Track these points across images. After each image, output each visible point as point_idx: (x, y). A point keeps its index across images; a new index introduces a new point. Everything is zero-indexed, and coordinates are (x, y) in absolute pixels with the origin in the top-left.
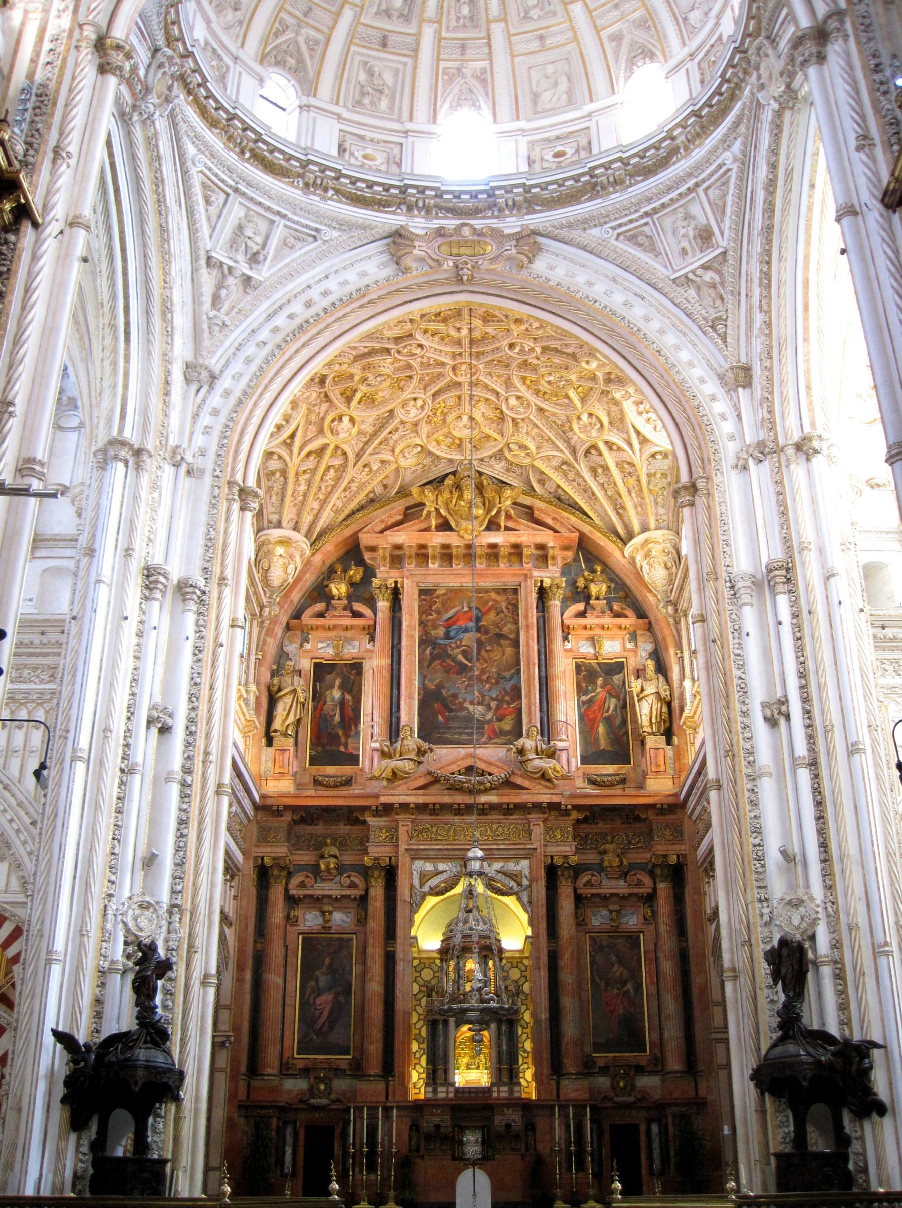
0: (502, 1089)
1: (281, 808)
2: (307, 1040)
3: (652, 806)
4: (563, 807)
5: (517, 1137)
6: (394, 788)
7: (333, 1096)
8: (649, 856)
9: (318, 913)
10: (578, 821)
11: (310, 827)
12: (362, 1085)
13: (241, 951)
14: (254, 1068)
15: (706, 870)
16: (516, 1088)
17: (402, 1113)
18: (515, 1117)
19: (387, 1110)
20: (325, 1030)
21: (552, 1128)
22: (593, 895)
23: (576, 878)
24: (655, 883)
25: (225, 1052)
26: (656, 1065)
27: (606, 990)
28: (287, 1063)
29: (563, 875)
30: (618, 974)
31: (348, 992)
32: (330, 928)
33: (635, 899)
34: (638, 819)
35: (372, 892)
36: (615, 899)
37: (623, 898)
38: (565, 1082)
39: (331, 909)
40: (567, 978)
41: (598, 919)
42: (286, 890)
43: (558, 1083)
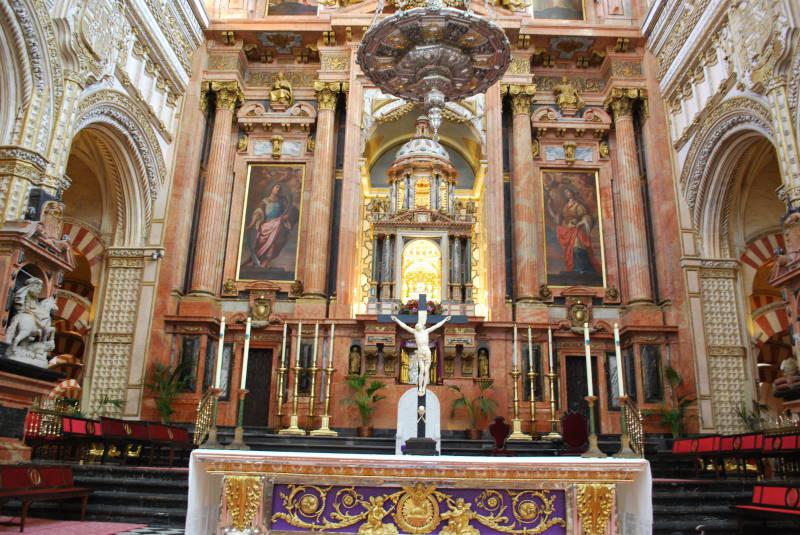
0: (454, 307)
1: (231, 33)
2: (251, 264)
3: (613, 41)
4: (521, 37)
5: (468, 360)
6: (345, 12)
7: (271, 317)
8: (604, 98)
9: (268, 143)
10: (535, 62)
11: (264, 65)
12: (301, 303)
13: (180, 167)
14: (188, 288)
15: (671, 100)
16: (469, 307)
17: (342, 333)
18: (468, 339)
19: (325, 328)
20: (269, 255)
21: (508, 354)
22: (551, 130)
23: (531, 111)
24: (613, 120)
25: (155, 263)
26: (615, 297)
27: (561, 224)
28: (227, 285)
29: (519, 104)
30: (572, 209)
31: (294, 217)
32: (279, 156)
33: (590, 137)
34: (596, 62)
35: (321, 116)
36: (571, 136)
37: (578, 134)
38: (520, 306)
39: (280, 137)
40: (523, 201)
41: (554, 154)
42: (235, 122)
43: (514, 307)
